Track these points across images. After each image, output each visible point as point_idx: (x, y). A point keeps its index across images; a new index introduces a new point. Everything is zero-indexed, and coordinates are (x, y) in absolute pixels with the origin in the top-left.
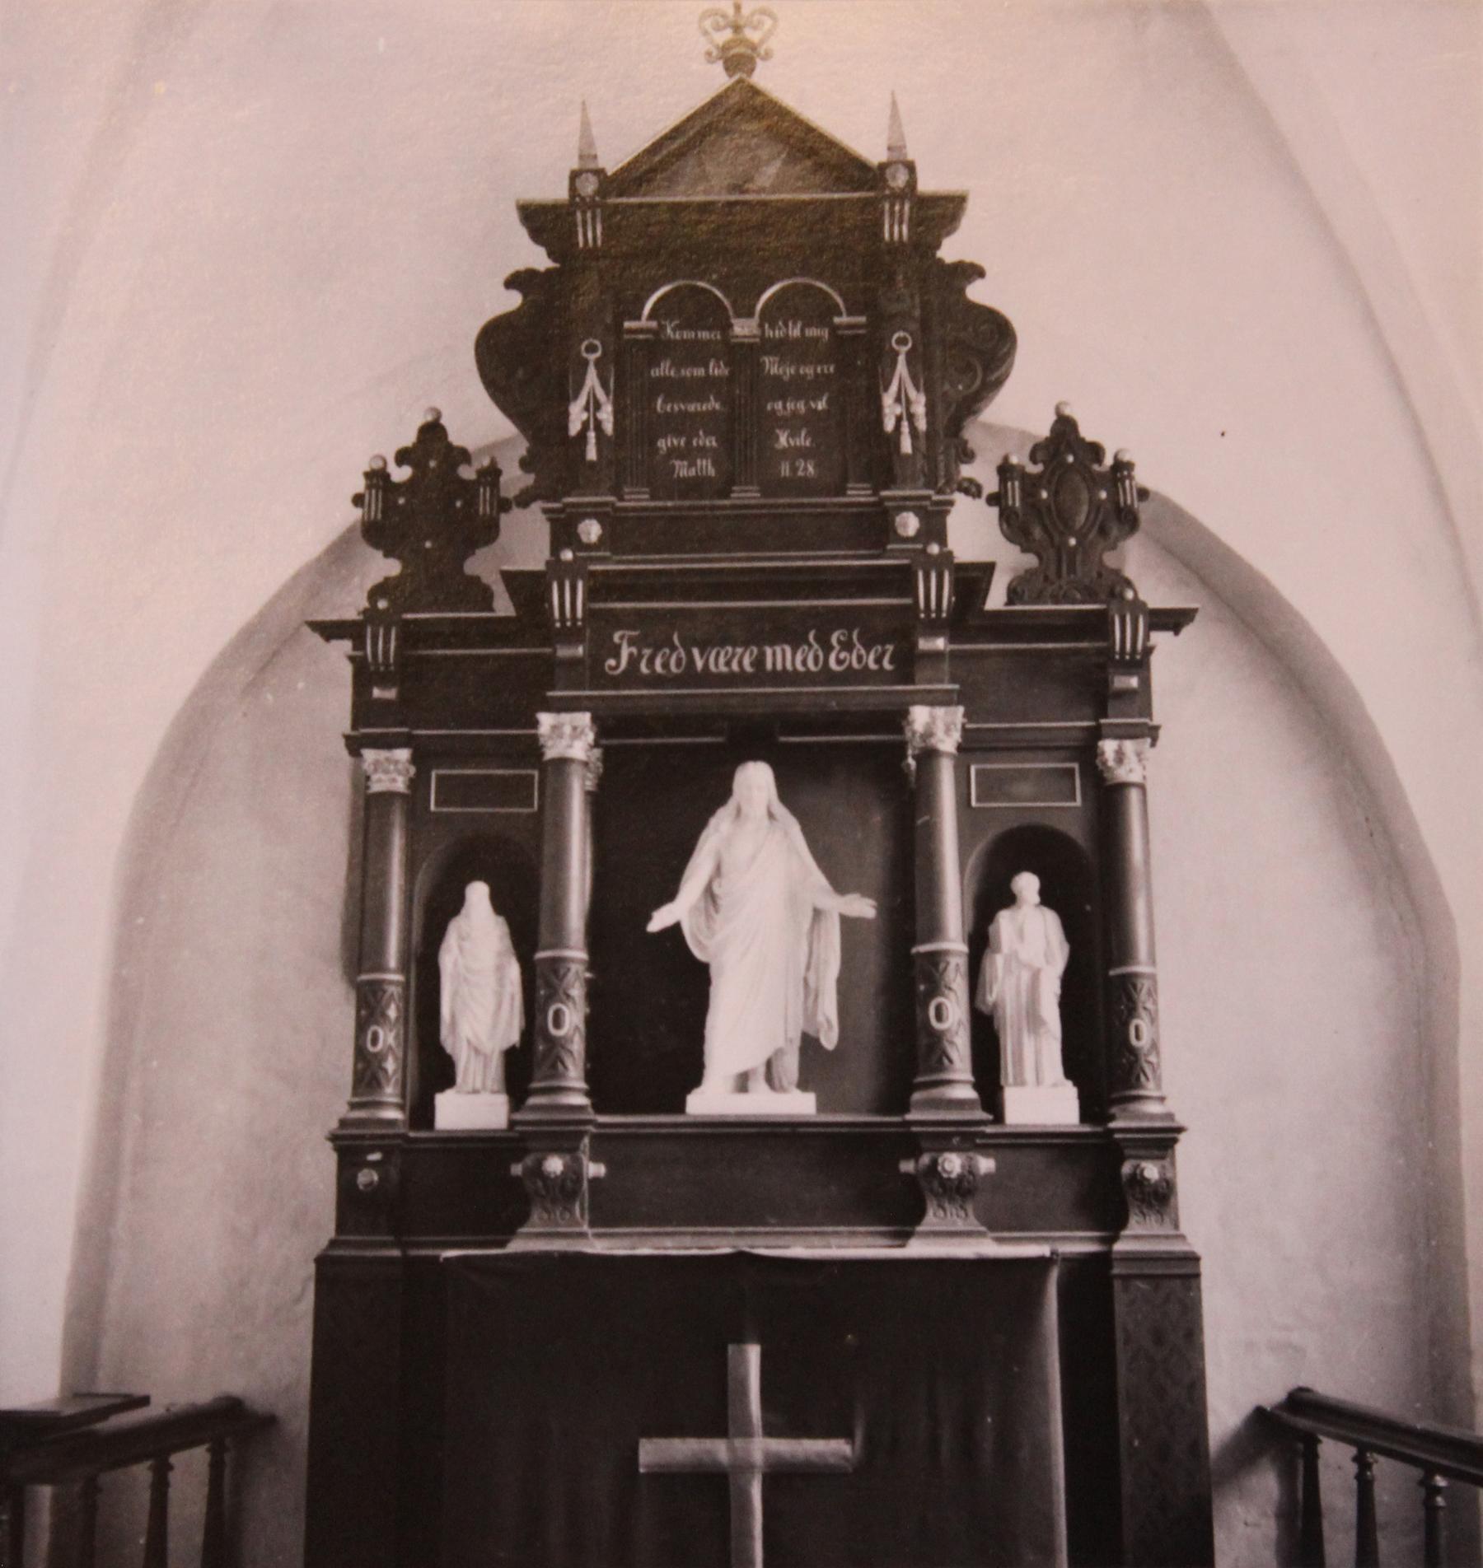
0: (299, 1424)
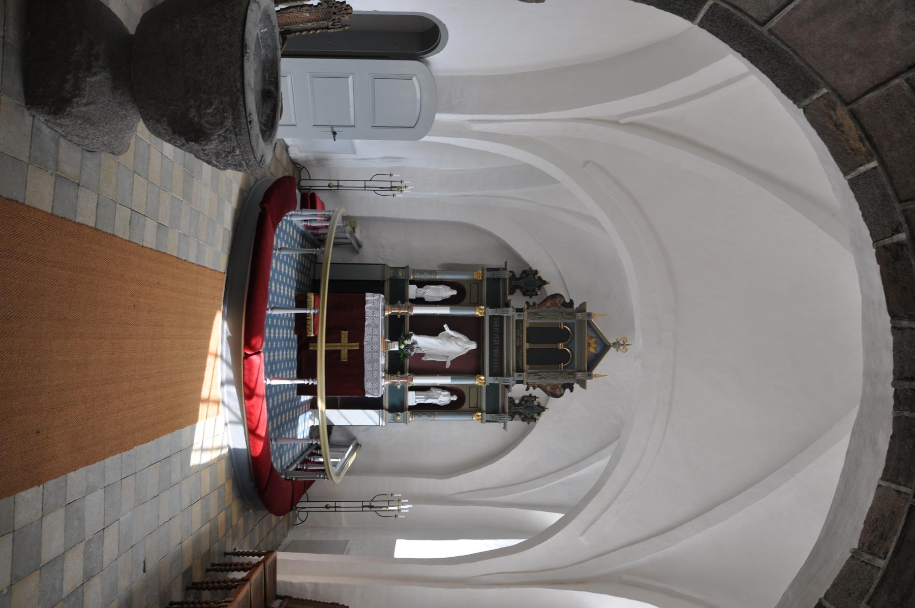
0: (355, 260)
